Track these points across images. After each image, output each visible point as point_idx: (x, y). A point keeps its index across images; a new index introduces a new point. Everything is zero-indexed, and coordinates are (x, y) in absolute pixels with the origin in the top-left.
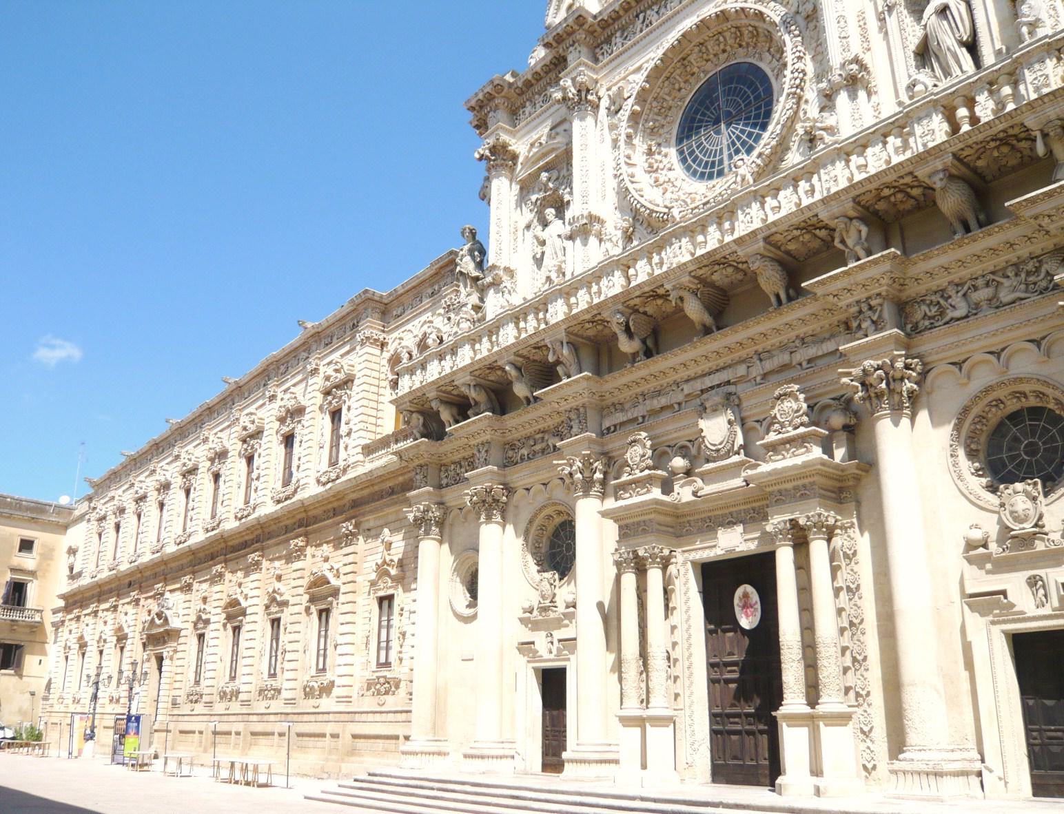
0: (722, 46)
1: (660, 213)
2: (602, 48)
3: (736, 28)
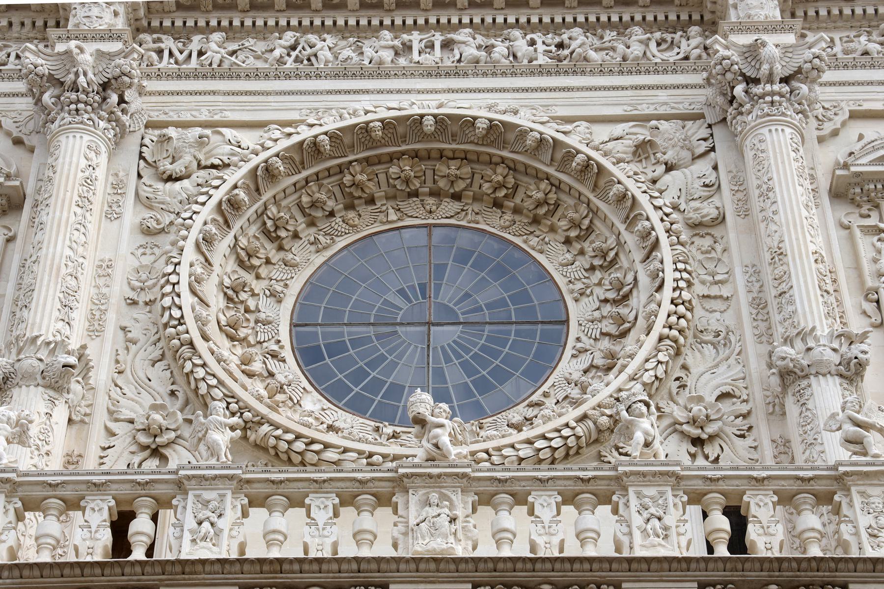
0: (460, 186)
1: (287, 431)
2: (159, 40)
3: (510, 169)
